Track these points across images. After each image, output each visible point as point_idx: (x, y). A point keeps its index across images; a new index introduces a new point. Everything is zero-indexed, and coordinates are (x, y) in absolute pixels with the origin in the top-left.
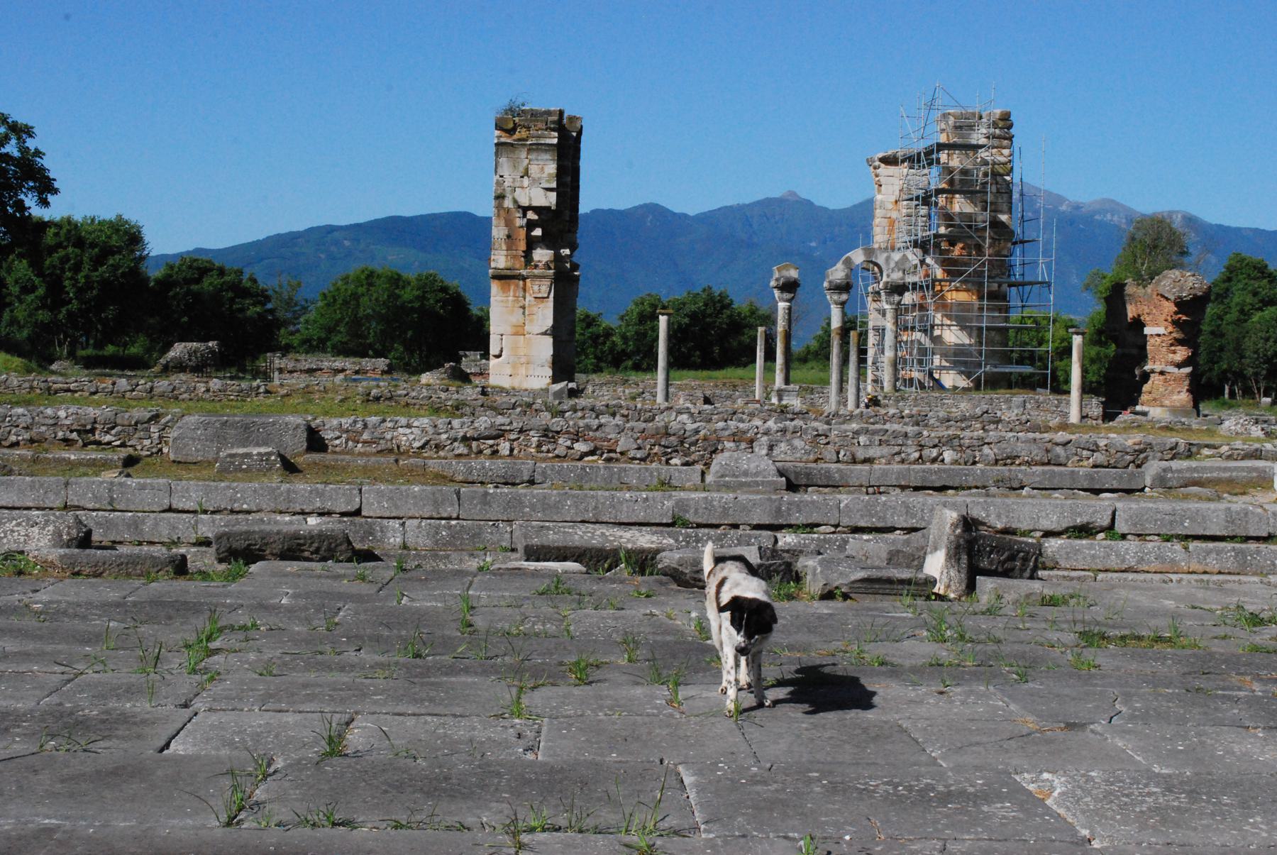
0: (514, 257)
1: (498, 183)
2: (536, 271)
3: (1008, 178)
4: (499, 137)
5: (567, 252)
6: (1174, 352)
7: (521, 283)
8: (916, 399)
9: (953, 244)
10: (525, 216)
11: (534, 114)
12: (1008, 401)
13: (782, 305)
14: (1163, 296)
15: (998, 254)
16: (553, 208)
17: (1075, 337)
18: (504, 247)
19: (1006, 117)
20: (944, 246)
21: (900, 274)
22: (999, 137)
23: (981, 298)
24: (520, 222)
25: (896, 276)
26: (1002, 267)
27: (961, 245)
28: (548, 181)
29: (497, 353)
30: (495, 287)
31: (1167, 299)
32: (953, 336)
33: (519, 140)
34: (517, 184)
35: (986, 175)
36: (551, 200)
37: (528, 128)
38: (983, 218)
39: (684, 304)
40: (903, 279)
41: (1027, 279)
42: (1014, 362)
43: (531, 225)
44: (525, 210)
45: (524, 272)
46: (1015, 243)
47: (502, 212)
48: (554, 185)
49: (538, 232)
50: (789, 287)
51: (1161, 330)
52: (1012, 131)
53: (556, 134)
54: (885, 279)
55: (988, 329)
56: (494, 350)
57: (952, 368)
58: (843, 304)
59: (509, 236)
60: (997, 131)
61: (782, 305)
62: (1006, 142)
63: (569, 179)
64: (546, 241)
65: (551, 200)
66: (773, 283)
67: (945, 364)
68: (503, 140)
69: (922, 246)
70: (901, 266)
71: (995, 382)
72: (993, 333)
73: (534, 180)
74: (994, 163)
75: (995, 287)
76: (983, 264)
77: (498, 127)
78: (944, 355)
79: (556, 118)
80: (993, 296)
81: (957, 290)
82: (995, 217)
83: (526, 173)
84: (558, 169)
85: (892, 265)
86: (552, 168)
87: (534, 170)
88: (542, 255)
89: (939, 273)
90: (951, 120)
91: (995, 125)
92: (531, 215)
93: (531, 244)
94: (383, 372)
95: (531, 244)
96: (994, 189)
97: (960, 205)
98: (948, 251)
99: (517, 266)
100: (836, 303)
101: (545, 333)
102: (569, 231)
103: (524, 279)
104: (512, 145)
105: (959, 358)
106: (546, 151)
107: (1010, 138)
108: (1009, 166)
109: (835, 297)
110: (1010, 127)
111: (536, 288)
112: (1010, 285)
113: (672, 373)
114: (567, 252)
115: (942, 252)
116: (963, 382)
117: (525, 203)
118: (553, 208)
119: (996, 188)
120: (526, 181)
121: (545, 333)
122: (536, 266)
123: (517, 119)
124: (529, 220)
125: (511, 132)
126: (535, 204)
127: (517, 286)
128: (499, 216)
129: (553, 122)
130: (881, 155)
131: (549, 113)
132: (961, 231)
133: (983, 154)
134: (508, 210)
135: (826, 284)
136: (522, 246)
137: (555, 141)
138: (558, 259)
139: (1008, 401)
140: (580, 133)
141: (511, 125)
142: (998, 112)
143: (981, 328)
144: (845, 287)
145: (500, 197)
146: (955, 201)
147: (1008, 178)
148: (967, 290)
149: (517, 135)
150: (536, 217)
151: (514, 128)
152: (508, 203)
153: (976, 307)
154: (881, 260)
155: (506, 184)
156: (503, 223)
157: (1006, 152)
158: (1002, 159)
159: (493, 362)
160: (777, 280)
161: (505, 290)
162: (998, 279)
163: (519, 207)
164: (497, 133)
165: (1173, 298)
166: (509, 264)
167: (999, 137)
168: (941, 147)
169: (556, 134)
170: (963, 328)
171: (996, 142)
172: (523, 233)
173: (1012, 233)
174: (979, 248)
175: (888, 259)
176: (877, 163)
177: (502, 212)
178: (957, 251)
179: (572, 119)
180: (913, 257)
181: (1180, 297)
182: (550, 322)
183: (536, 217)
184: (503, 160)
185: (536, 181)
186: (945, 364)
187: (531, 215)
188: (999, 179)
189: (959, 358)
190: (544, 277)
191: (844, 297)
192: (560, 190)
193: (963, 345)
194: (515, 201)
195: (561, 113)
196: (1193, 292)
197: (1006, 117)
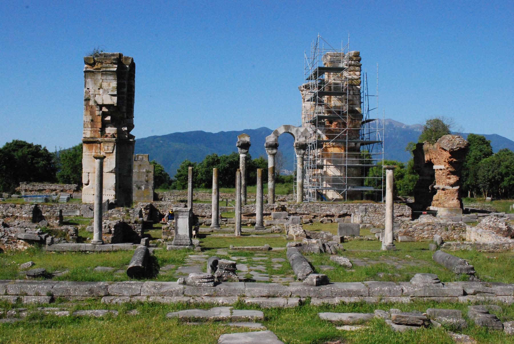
0: (95, 131)
1: (86, 92)
2: (106, 139)
3: (359, 87)
4: (86, 68)
5: (126, 129)
6: (449, 178)
7: (99, 145)
8: (306, 207)
9: (331, 123)
10: (101, 109)
11: (106, 56)
12: (358, 207)
13: (242, 156)
14: (443, 149)
15: (355, 127)
16: (115, 105)
17: (387, 171)
18: (90, 126)
19: (357, 55)
20: (327, 123)
21: (304, 139)
22: (354, 65)
23: (345, 151)
24: (98, 113)
25: (302, 140)
26: (355, 133)
27: (336, 123)
28: (112, 91)
29: (86, 183)
30: (85, 147)
31: (445, 150)
32: (332, 171)
33: (97, 69)
34: (96, 93)
35: (346, 85)
36: (114, 101)
37: (102, 63)
38: (346, 108)
39: (227, 158)
40: (305, 141)
41: (372, 139)
42: (362, 185)
43: (104, 115)
44: (101, 106)
45: (100, 139)
46: (363, 123)
47: (88, 108)
48: (115, 93)
49: (108, 118)
50: (245, 146)
51: (442, 167)
52: (361, 62)
53: (116, 66)
54: (296, 141)
55: (349, 167)
56: (84, 181)
57: (331, 188)
58: (274, 155)
59: (92, 121)
60: (353, 62)
61: (242, 156)
62: (357, 68)
63: (125, 90)
64: (114, 123)
65: (114, 101)
66: (237, 145)
67: (328, 186)
68: (88, 69)
69: (313, 122)
70: (305, 134)
71: (352, 196)
72: (353, 169)
73: (105, 90)
74: (352, 80)
75: (353, 144)
76: (346, 132)
77: (86, 63)
78: (328, 182)
79: (116, 57)
80: (351, 149)
81: (333, 147)
82: (352, 108)
83: (101, 87)
84: (118, 84)
85: (300, 134)
86: (114, 84)
87: (105, 85)
88: (111, 130)
89: (325, 138)
90: (329, 58)
91: (351, 59)
92: (105, 109)
93: (105, 125)
94: (74, 191)
95: (105, 125)
96: (351, 93)
97: (334, 102)
98: (329, 126)
99: (97, 136)
100: (271, 155)
101: (111, 172)
102: (127, 118)
103: (100, 143)
104: (93, 72)
105: (335, 183)
106: (111, 75)
107: (360, 66)
108: (359, 80)
109: (270, 151)
110: (359, 60)
111: (106, 148)
112: (362, 144)
113: (221, 190)
114: (126, 129)
115: (326, 126)
116: (337, 196)
117: (100, 102)
118: (115, 105)
119: (353, 92)
120: (101, 91)
121: (111, 172)
122: (107, 136)
123: (96, 58)
124: (103, 112)
125: (92, 65)
126: (105, 103)
127: (97, 147)
128: (87, 110)
129: (114, 59)
130: (304, 85)
131: (113, 55)
132: (335, 115)
133: (345, 74)
134: (92, 107)
135: (265, 145)
136: (99, 125)
137: (115, 69)
138: (119, 132)
139: (358, 207)
140: (133, 65)
141: (92, 62)
142: (353, 52)
143: (345, 167)
144: (274, 146)
145: (87, 100)
146: (332, 99)
147: (359, 87)
148: (338, 147)
149: (96, 67)
150: (107, 110)
151: (94, 64)
152: (91, 103)
153: (344, 155)
154: (293, 132)
155: (91, 93)
156: (89, 113)
157: (358, 73)
158: (356, 77)
159: (85, 187)
160: (238, 143)
161: (90, 149)
162: (354, 140)
163: (98, 105)
164: (86, 66)
165: (448, 150)
166: (92, 135)
167: (354, 65)
168: (322, 70)
169: (116, 66)
170: (337, 167)
171: (352, 68)
172: (100, 119)
173: (362, 116)
174: (345, 125)
175: (297, 131)
176: (302, 89)
177: (88, 108)
178: (333, 127)
179: (127, 58)
180: (310, 129)
181: (452, 149)
182: (114, 166)
183: (107, 110)
184: (89, 80)
186: (328, 186)
187: (105, 109)
188: (354, 87)
189: (335, 183)
190: (110, 142)
191: (274, 151)
192: (119, 95)
193: (335, 176)
194: (95, 102)
195: (121, 55)
196: (459, 146)
197: (357, 55)
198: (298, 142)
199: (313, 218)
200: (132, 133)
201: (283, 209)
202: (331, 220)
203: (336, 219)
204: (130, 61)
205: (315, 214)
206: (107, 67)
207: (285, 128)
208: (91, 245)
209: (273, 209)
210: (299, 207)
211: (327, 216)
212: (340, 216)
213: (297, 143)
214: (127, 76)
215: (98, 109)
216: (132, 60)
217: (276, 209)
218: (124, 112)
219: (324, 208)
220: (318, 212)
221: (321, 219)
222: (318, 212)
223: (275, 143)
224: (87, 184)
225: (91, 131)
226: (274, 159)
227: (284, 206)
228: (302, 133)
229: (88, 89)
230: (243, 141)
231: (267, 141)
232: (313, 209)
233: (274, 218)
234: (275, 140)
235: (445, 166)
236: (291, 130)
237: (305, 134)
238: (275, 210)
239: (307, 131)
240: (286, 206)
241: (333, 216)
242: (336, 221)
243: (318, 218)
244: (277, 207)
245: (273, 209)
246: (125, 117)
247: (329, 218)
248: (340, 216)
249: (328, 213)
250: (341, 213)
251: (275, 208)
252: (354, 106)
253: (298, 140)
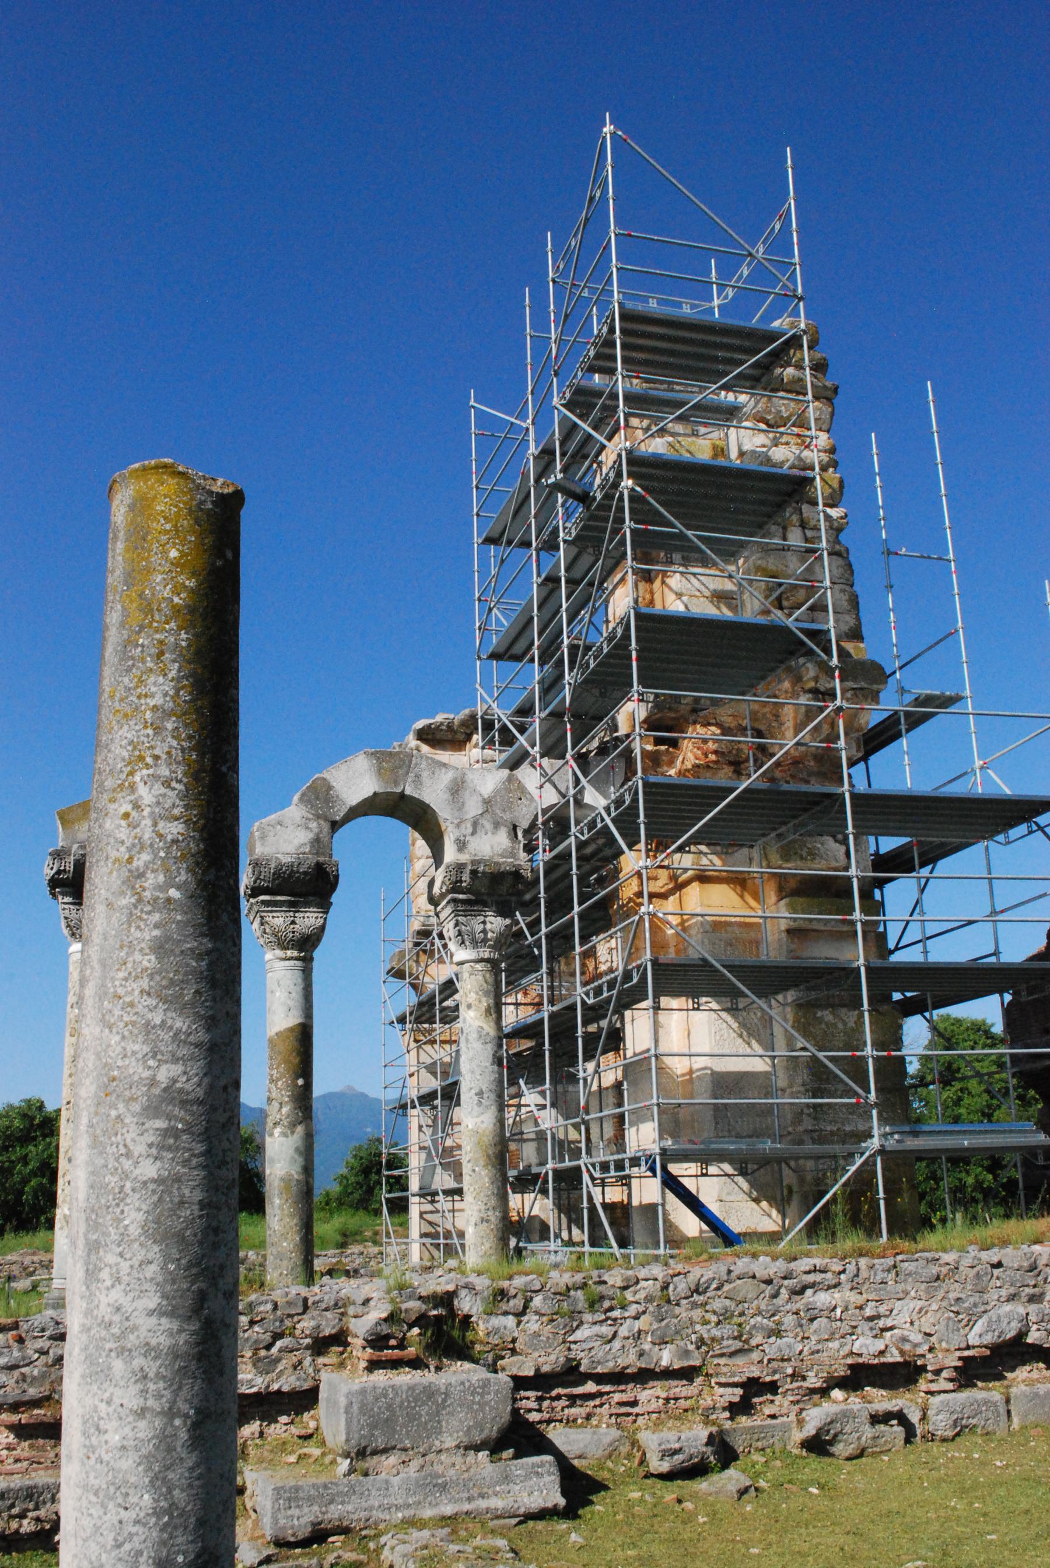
8: (665, 1298)
81: (703, 878)
85: (473, 808)
100: (283, 945)
105: (721, 1123)
109: (279, 920)
191: (308, 919)
198: (464, 858)
199: (736, 1409)
201: (445, 1333)
202: (901, 1417)
203: (937, 1404)
205: (748, 1368)
207: (380, 772)
209: (340, 1339)
210: (593, 1304)
211: (859, 1377)
212: (973, 1371)
213: (460, 867)
217: (378, 1341)
219: (822, 1299)
220: (773, 1347)
221: (816, 1416)
222: (773, 1347)
223: (312, 860)
226: (307, 973)
227: (446, 1300)
228: (487, 802)
231: (260, 850)
232: (725, 1317)
233: (361, 1453)
234: (317, 840)
236: (418, 780)
237: (508, 807)
238: (360, 1353)
239: (522, 789)
240: (465, 1304)
241: (903, 1374)
242: (940, 1423)
243: (781, 1403)
244: (378, 1312)
245: (340, 1339)
247: (881, 1400)
248: (973, 1371)
249: (867, 1347)
250: (979, 1336)
251: (361, 1326)
253: (461, 845)
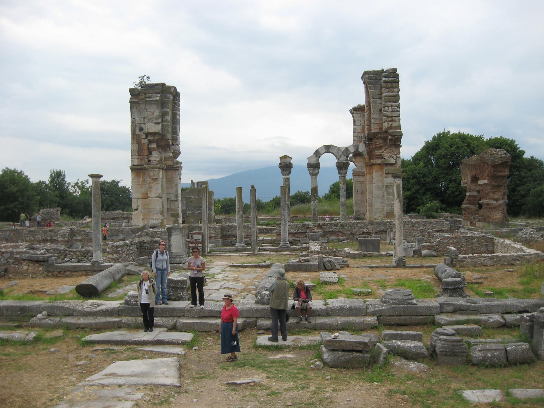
0: (142, 159)
18: (137, 154)
21: (345, 158)
28: (156, 119)
43: (150, 142)
44: (147, 135)
45: (146, 166)
48: (160, 121)
49: (154, 146)
51: (486, 181)
62: (394, 85)
63: (169, 117)
68: (133, 100)
85: (341, 153)
99: (144, 163)
102: (173, 144)
126: (151, 131)
136: (146, 153)
141: (137, 93)
149: (140, 97)
155: (137, 122)
179: (170, 87)
183: (152, 138)
184: (135, 110)
185: (150, 120)
200: (179, 159)
204: (172, 90)
206: (150, 97)
208: (89, 264)
214: (170, 105)
215: (144, 136)
216: (175, 88)
218: (169, 139)
224: (137, 210)
225: (138, 159)
229: (134, 119)
230: (285, 163)
235: (488, 180)
246: (171, 144)
252: (393, 123)
